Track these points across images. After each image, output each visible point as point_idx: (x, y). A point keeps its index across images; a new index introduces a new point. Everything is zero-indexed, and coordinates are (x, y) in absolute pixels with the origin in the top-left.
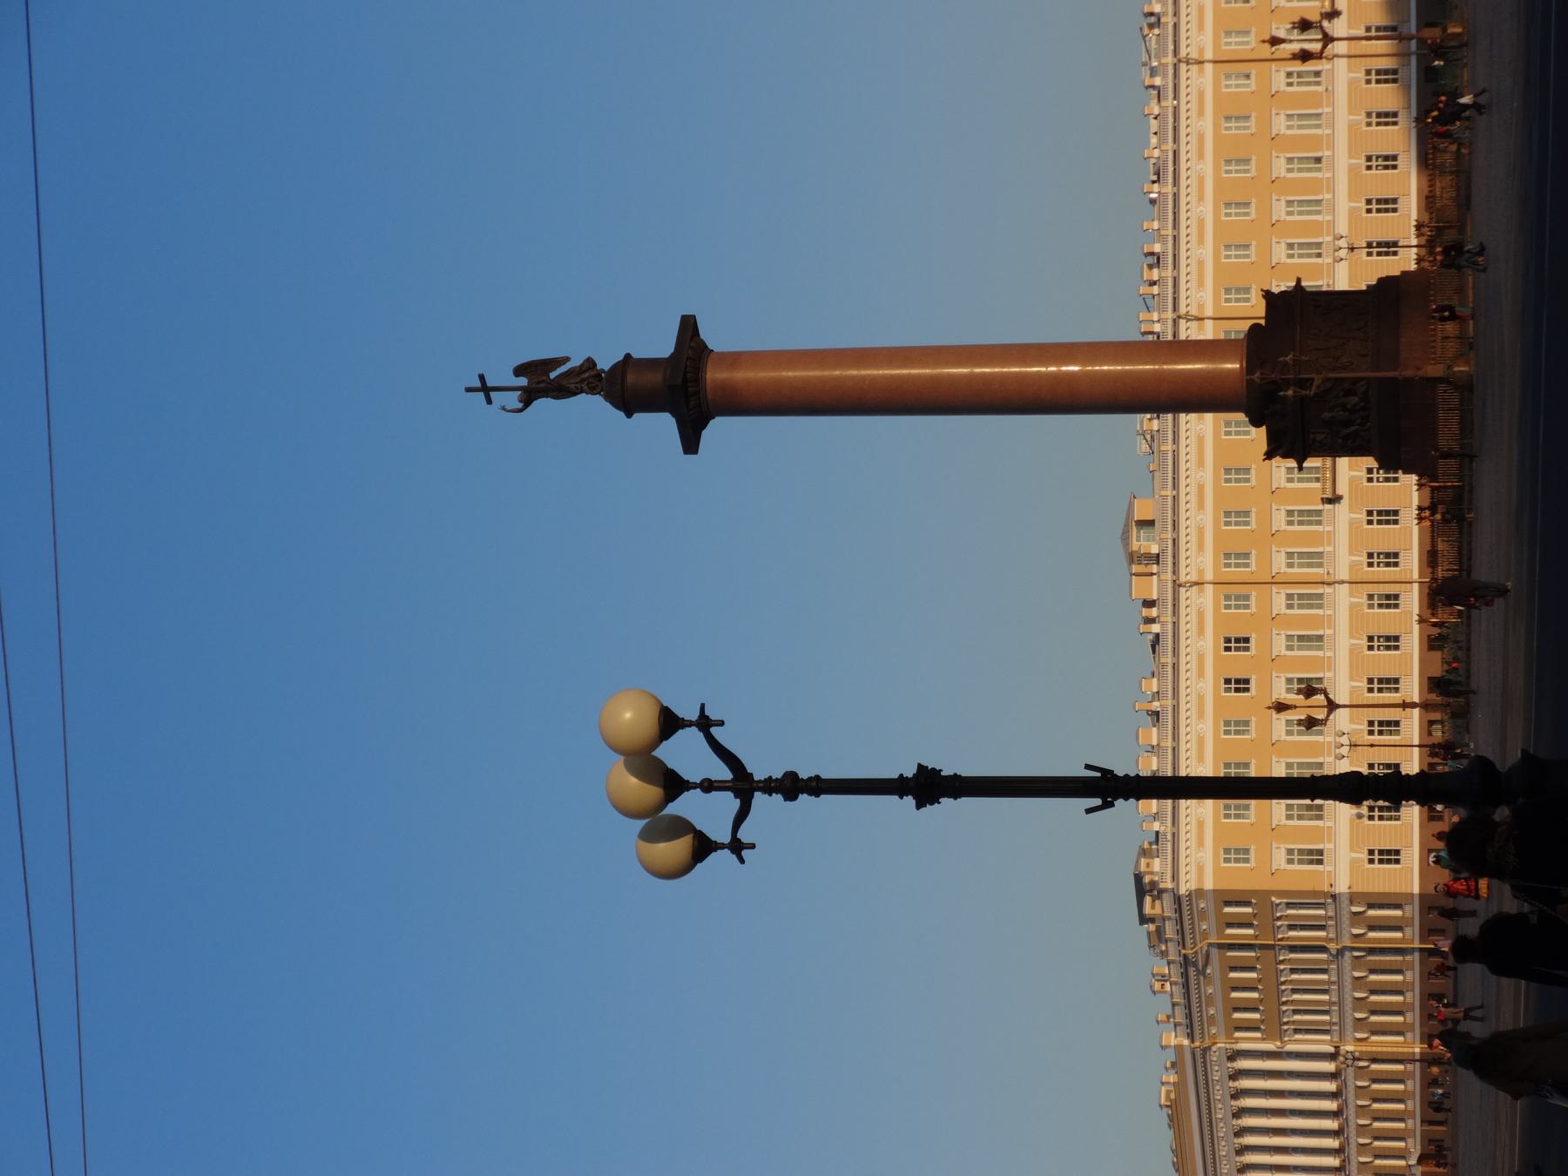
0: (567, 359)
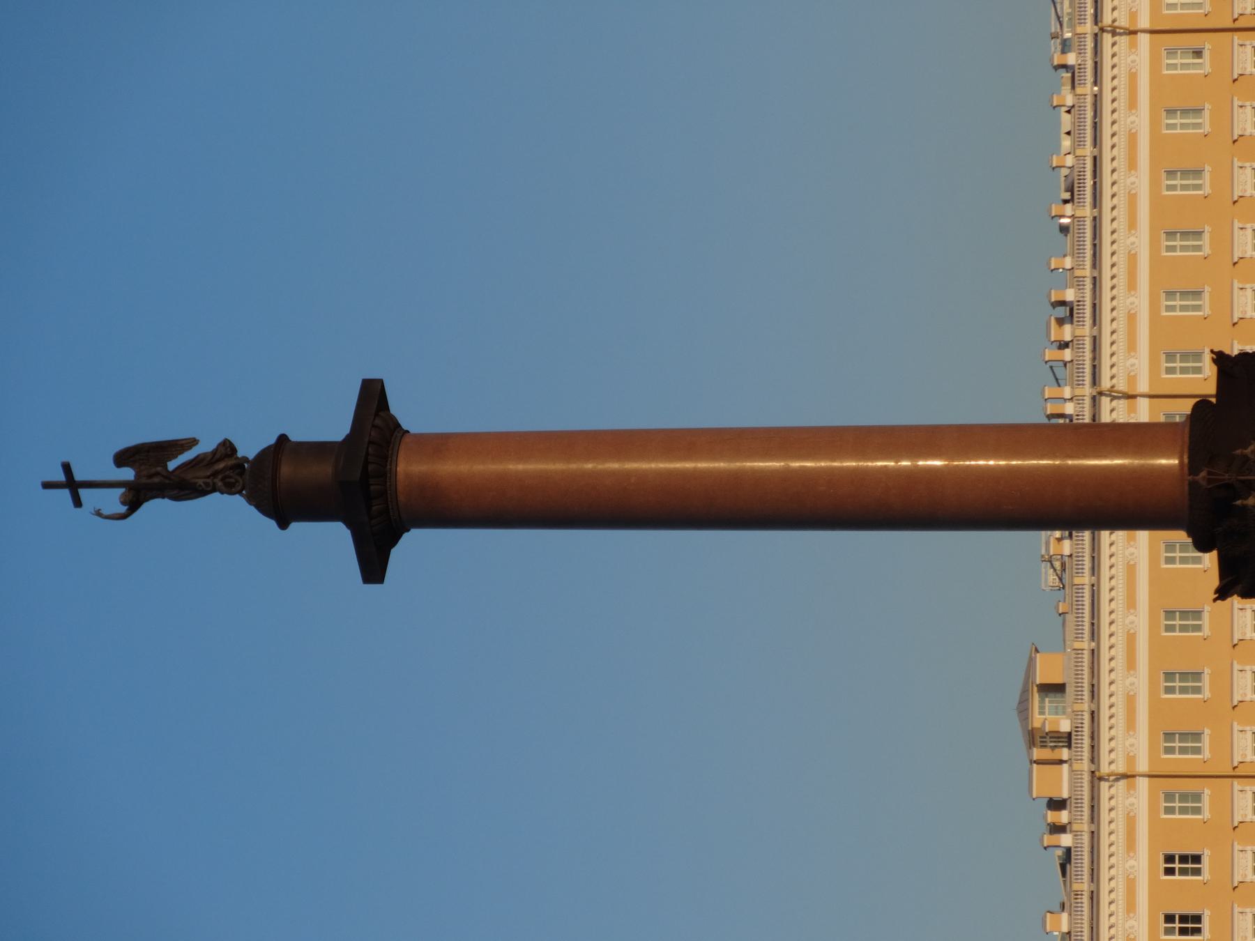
0: (193, 442)
